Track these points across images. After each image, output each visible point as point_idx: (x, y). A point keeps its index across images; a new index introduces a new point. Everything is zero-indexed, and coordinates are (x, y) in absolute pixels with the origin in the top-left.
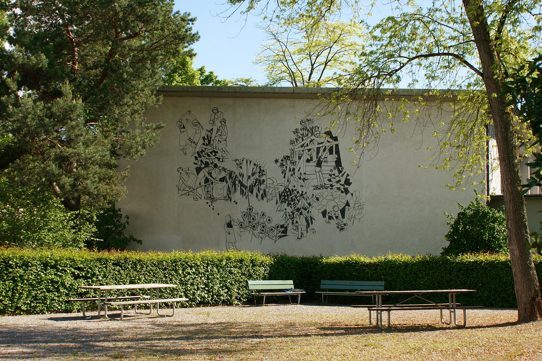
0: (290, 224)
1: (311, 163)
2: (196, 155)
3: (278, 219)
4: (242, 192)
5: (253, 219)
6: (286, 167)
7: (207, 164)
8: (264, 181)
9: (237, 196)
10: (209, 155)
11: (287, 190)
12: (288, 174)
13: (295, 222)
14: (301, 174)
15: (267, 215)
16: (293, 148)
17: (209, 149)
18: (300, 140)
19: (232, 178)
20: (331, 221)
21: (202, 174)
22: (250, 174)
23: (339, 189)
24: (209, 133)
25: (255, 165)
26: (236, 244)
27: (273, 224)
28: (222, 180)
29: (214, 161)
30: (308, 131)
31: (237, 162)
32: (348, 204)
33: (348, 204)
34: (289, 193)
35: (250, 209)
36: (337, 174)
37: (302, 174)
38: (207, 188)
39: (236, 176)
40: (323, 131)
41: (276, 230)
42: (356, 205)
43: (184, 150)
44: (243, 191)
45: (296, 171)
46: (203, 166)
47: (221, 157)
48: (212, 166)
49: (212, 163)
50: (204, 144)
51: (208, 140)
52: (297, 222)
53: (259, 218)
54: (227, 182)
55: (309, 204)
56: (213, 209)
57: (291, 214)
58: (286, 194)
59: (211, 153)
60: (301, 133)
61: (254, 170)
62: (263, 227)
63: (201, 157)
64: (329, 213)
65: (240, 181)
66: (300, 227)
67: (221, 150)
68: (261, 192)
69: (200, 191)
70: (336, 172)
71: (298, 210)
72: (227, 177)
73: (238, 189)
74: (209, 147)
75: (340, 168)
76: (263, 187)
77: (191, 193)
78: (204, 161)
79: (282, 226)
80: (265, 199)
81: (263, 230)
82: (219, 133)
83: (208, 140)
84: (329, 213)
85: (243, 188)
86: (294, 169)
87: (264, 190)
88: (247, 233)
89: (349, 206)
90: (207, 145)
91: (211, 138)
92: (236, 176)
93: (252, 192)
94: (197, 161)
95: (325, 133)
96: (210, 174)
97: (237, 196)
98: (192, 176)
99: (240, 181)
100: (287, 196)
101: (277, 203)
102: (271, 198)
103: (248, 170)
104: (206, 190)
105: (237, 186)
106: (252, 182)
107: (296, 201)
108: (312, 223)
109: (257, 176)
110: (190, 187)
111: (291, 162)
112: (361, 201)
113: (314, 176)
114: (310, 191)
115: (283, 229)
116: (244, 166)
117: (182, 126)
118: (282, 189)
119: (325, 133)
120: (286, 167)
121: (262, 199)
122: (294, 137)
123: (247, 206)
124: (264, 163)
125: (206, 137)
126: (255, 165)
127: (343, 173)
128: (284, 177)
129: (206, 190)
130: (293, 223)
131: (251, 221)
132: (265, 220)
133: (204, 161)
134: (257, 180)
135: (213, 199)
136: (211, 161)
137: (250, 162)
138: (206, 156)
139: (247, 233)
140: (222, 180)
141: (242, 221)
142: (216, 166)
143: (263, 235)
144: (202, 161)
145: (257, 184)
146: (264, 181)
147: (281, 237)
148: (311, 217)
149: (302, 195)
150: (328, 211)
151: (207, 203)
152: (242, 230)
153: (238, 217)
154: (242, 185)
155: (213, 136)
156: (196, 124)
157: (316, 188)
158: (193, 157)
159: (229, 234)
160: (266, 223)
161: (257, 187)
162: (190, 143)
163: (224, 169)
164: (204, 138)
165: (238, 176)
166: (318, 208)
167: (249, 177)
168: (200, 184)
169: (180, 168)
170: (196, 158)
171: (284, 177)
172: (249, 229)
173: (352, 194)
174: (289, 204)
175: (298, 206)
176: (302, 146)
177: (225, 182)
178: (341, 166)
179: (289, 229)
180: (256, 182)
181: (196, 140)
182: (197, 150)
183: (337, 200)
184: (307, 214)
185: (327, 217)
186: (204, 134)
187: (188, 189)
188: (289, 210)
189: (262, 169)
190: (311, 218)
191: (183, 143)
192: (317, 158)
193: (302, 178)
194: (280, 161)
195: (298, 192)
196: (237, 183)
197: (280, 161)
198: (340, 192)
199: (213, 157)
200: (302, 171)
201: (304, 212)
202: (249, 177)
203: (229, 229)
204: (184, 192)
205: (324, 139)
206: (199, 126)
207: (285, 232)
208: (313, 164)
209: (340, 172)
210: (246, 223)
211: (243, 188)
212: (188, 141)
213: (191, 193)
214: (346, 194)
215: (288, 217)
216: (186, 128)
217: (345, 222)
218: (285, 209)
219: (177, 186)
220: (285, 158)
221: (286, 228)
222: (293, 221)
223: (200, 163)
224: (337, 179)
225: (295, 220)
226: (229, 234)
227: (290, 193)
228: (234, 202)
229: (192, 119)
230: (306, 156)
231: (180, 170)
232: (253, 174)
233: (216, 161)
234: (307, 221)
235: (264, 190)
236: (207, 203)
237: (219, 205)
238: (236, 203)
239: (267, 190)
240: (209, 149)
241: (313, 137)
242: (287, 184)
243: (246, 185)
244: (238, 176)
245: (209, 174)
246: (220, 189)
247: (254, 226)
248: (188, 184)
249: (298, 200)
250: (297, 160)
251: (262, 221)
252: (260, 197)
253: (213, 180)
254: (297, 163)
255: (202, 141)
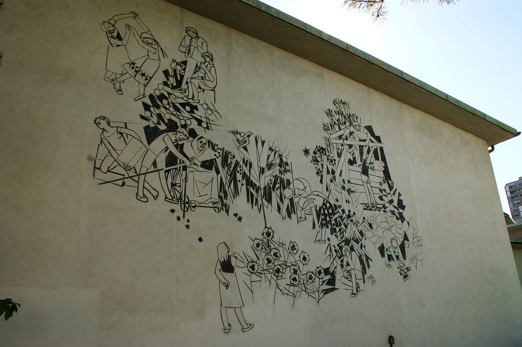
0: (339, 267)
1: (354, 167)
2: (148, 101)
3: (319, 257)
4: (250, 198)
5: (275, 254)
6: (322, 165)
7: (172, 127)
8: (289, 183)
9: (240, 203)
10: (177, 109)
11: (328, 205)
12: (327, 178)
13: (345, 263)
14: (343, 180)
15: (301, 247)
16: (328, 137)
17: (177, 97)
18: (337, 127)
19: (229, 166)
20: (392, 263)
21: (159, 143)
22: (264, 165)
23: (393, 212)
24: (179, 68)
25: (271, 149)
26: (245, 310)
27: (311, 267)
28: (208, 165)
29: (188, 122)
30: (345, 117)
31: (238, 136)
32: (406, 238)
33: (406, 238)
34: (330, 211)
35: (268, 234)
36: (388, 191)
37: (346, 181)
38: (173, 177)
39: (237, 163)
40: (363, 125)
41: (317, 279)
42: (415, 240)
43: (116, 83)
44: (252, 195)
45: (337, 174)
46: (163, 127)
47: (204, 120)
48: (186, 132)
49: (185, 126)
50: (166, 84)
51: (176, 79)
52: (348, 264)
53: (286, 254)
54: (218, 172)
55: (361, 233)
56: (188, 227)
57: (337, 248)
58: (326, 212)
59: (183, 105)
60: (337, 117)
61: (271, 159)
62: (295, 272)
63: (158, 107)
64: (387, 250)
65: (244, 175)
66: (353, 272)
67: (205, 107)
68: (287, 202)
69: (153, 179)
70: (385, 186)
71: (347, 242)
72: (219, 161)
73: (243, 190)
74: (176, 93)
75: (390, 182)
76: (287, 193)
77: (128, 182)
78: (167, 117)
79: (327, 271)
80: (293, 216)
81: (295, 279)
82: (200, 74)
83: (176, 79)
84: (387, 250)
85: (251, 189)
86: (333, 172)
87: (291, 200)
88: (264, 284)
89: (408, 240)
90: (173, 88)
91: (182, 77)
92: (237, 163)
93: (269, 200)
94: (147, 114)
95: (365, 127)
96: (180, 147)
97: (240, 203)
98: (133, 143)
99: (244, 175)
100: (328, 216)
101: (314, 228)
102: (303, 217)
103: (259, 156)
104: (170, 180)
105: (239, 184)
106: (267, 180)
107: (343, 226)
108: (369, 266)
109: (276, 170)
110: (127, 168)
111: (328, 159)
112: (418, 235)
113: (361, 189)
114: (360, 213)
115: (328, 277)
116: (251, 146)
117: (115, 34)
118: (319, 202)
119: (365, 127)
120: (322, 165)
121: (289, 216)
122: (327, 120)
123: (261, 228)
124: (287, 151)
125: (171, 73)
126: (271, 149)
127: (394, 189)
128: (321, 182)
129: (170, 180)
130: (342, 266)
131: (270, 258)
132: (297, 258)
133: (167, 117)
134: (276, 177)
135: (186, 204)
136: (183, 123)
137: (263, 143)
138: (172, 109)
139: (264, 284)
140: (208, 165)
141: (255, 258)
142: (193, 134)
143: (296, 289)
144: (159, 116)
145: (278, 185)
146: (289, 183)
147: (326, 292)
148: (366, 256)
149: (349, 216)
150: (386, 246)
151: (173, 211)
152: (254, 277)
153: (243, 249)
154: (249, 183)
155: (188, 74)
156: (150, 41)
157: (367, 207)
158: (140, 103)
159: (227, 286)
160: (300, 264)
161: (278, 192)
162: (132, 72)
163: (213, 146)
164: (166, 73)
165: (241, 163)
166: (374, 240)
167: (262, 171)
168: (155, 164)
169: (104, 118)
170: (147, 107)
171: (321, 182)
172: (269, 276)
173: (408, 223)
174: (333, 231)
175: (348, 235)
176: (340, 137)
177: (213, 172)
178: (391, 180)
179: (338, 276)
180: (275, 182)
181: (148, 70)
182: (150, 90)
183: (393, 230)
184: (359, 249)
185: (386, 256)
186: (166, 64)
187: (123, 172)
188: (335, 241)
189: (284, 160)
190: (367, 258)
191: (115, 67)
192: (361, 161)
193: (346, 188)
194: (311, 152)
195: (343, 211)
196: (239, 177)
197: (311, 152)
198: (395, 218)
199: (187, 115)
200: (344, 176)
201: (356, 247)
202: (262, 171)
203: (227, 275)
204: (110, 177)
205: (364, 134)
206: (156, 46)
207: (332, 282)
208: (357, 168)
209: (391, 188)
210: (262, 263)
211: (251, 189)
212: (127, 67)
213: (128, 182)
214: (402, 222)
215: (335, 254)
216: (125, 41)
217: (407, 265)
218: (329, 239)
219: (90, 158)
220: (319, 150)
221: (333, 274)
222: (342, 261)
223: (155, 119)
224: (389, 198)
225: (345, 260)
226: (227, 286)
227: (332, 210)
228: (236, 215)
229: (140, 30)
230: (347, 156)
231: (103, 124)
232: (270, 166)
233: (194, 125)
234: (361, 262)
235: (291, 200)
236: (173, 211)
237: (202, 219)
238: (240, 219)
239: (296, 200)
240: (177, 97)
241: (352, 129)
242: (327, 194)
243: (258, 184)
244: (241, 163)
245: (177, 146)
246: (202, 185)
247: (278, 271)
248: (124, 158)
249: (344, 224)
250: (336, 157)
251: (292, 260)
252: (284, 211)
253: (187, 163)
254: (337, 162)
255: (161, 77)
